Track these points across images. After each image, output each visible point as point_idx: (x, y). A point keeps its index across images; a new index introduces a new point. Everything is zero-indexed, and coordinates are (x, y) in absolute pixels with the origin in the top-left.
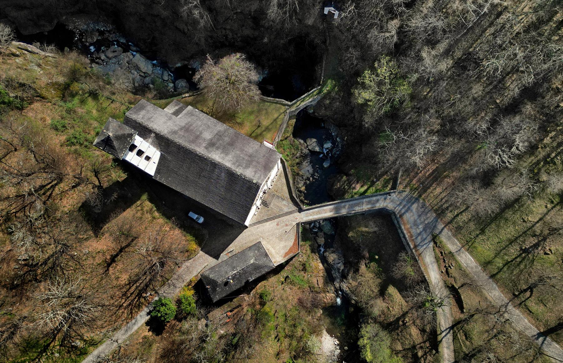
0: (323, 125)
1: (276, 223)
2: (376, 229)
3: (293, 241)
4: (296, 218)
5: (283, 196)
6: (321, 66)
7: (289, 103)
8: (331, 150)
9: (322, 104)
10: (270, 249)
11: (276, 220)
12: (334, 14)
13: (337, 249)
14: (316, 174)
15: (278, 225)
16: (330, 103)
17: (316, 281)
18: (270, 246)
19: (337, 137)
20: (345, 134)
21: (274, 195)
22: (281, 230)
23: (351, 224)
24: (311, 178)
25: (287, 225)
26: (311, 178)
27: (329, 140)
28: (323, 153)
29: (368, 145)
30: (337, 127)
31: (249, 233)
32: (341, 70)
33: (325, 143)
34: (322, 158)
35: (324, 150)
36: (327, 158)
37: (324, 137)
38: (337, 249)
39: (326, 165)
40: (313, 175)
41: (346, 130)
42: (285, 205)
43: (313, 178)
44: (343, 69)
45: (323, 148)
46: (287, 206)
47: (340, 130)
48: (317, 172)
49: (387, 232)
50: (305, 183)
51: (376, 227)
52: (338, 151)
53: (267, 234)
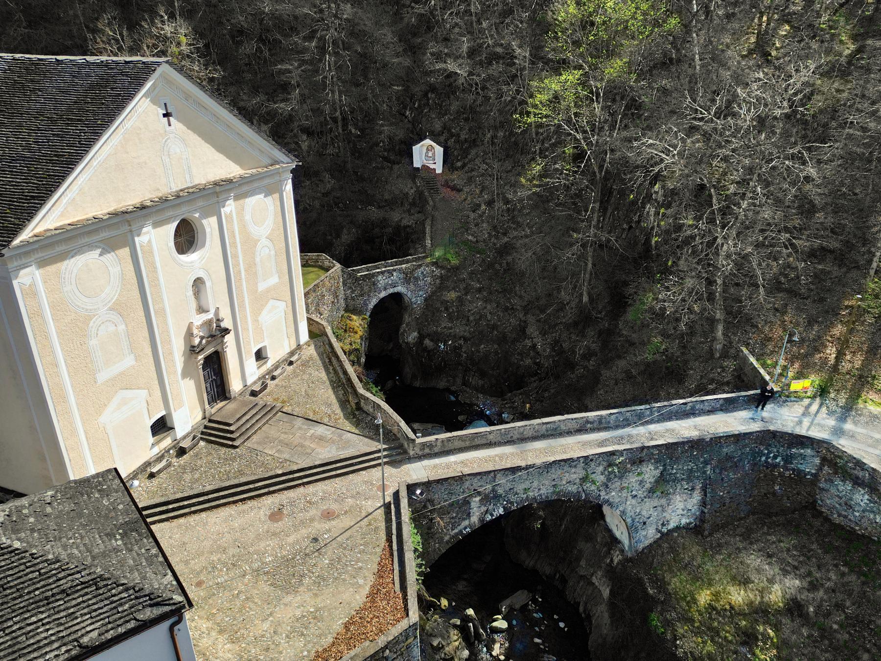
9: (438, 305)
12: (434, 169)
22: (290, 540)
23: (662, 585)
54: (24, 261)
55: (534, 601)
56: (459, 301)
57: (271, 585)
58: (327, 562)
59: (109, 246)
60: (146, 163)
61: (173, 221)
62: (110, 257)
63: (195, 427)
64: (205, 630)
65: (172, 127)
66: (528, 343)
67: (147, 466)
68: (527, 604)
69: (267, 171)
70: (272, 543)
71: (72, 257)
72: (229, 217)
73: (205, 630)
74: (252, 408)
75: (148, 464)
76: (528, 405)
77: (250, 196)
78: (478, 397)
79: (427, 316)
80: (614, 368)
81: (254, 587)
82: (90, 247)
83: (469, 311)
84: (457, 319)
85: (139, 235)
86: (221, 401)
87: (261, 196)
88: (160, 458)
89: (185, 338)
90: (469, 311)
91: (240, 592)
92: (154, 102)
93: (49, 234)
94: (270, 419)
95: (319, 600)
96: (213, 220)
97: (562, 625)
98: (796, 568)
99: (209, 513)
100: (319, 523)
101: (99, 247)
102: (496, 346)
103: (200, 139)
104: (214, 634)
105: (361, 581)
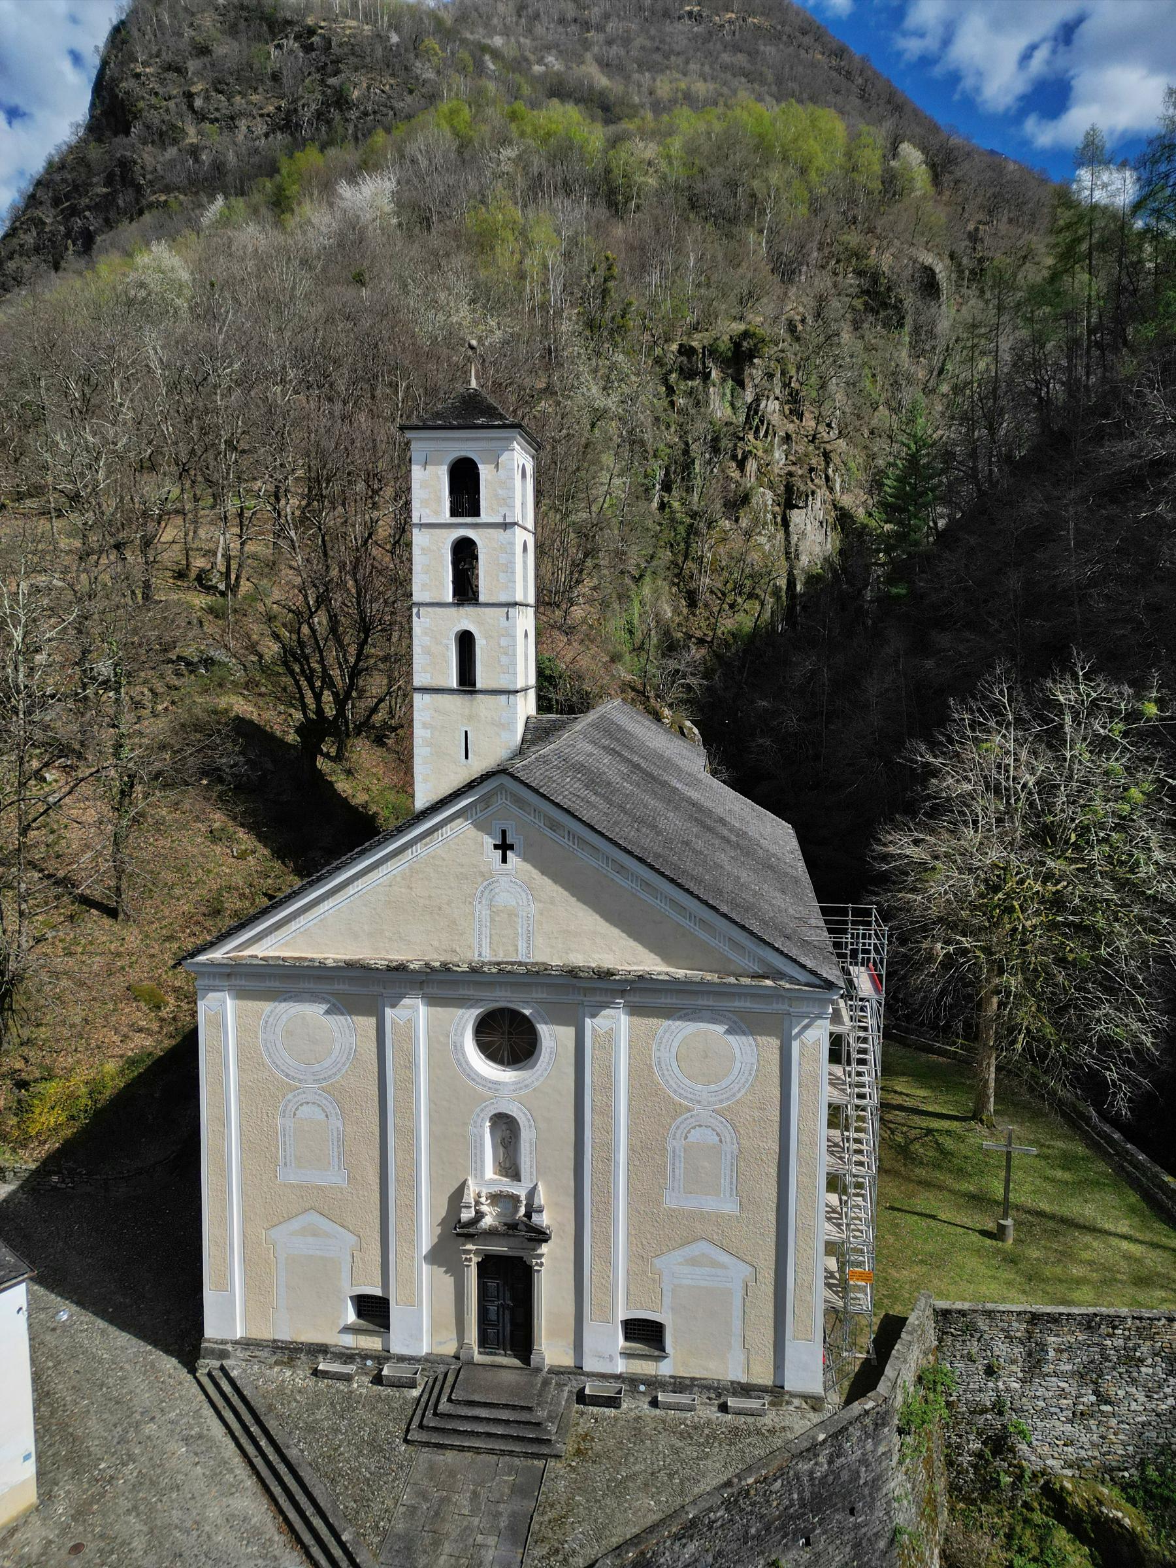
5: (560, 1521)
31: (144, 1396)
54: (217, 983)
59: (343, 1005)
60: (440, 908)
61: (471, 1007)
62: (342, 1021)
63: (431, 1358)
65: (509, 865)
67: (319, 1351)
69: (730, 984)
71: (285, 1000)
72: (608, 1042)
74: (514, 1407)
75: (322, 1350)
77: (680, 1018)
82: (314, 997)
85: (393, 1006)
86: (516, 1357)
87: (720, 1029)
88: (347, 1357)
89: (450, 1198)
92: (480, 826)
93: (255, 962)
94: (511, 1453)
96: (567, 1033)
99: (258, 1489)
101: (328, 1002)
103: (566, 893)
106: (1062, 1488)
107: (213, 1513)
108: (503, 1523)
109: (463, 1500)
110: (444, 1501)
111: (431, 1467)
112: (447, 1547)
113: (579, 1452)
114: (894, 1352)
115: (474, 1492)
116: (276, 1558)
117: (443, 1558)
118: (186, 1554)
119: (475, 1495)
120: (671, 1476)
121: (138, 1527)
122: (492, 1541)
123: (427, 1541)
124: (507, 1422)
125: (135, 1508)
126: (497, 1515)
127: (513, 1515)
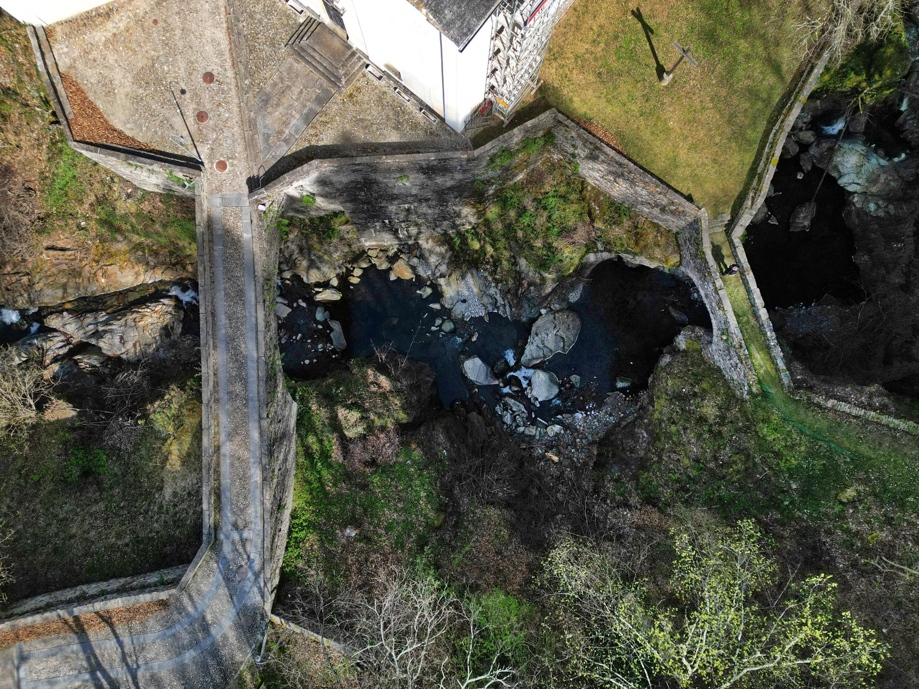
0: (620, 385)
1: (215, 69)
2: (168, 492)
3: (129, 131)
4: (222, 165)
6: (883, 409)
7: (739, 232)
8: (520, 395)
9: (705, 385)
10: (110, 25)
11: (230, 74)
13: (173, 345)
14: (448, 326)
15: (209, 77)
16: (702, 420)
17: (60, 244)
18: (122, 25)
19: (566, 427)
20: (570, 458)
21: (334, 80)
24: (436, 306)
25: (201, 116)
26: (436, 306)
27: (558, 396)
28: (518, 366)
29: (505, 532)
30: (601, 434)
32: (850, 493)
33: (552, 380)
34: (503, 357)
35: (530, 372)
36: (497, 376)
37: (575, 379)
38: (173, 345)
39: (474, 368)
40: (446, 313)
41: (585, 464)
42: (286, 124)
43: (435, 314)
44: (852, 503)
45: (535, 367)
46: (280, 132)
47: (591, 444)
48: (453, 332)
49: (142, 534)
50: (420, 282)
51: (175, 494)
52: (514, 419)
53: (176, 21)
55: (334, 351)
56: (701, 417)
57: (142, 68)
58: (154, 107)
64: (118, 25)
66: (634, 500)
68: (332, 344)
70: (182, 73)
73: (118, 25)
76: (556, 459)
78: (611, 415)
79: (699, 366)
80: (524, 568)
81: (143, 57)
83: (685, 429)
84: (682, 409)
90: (685, 429)
91: (141, 47)
95: (123, 96)
97: (307, 362)
98: (175, 506)
100: (195, 109)
102: (642, 453)
104: (115, 31)
105: (129, 126)
106: (586, 187)
107: (208, 33)
108: (305, 111)
109: (296, 91)
110: (289, 87)
111: (290, 68)
112: (281, 109)
113: (351, 96)
114: (501, 136)
115: (302, 90)
116: (225, 70)
117: (278, 113)
118: (194, 48)
119: (301, 92)
120: (378, 129)
121: (179, 24)
122: (298, 116)
123: (275, 102)
124: (325, 67)
125: (178, 13)
126: (305, 106)
127: (311, 110)
